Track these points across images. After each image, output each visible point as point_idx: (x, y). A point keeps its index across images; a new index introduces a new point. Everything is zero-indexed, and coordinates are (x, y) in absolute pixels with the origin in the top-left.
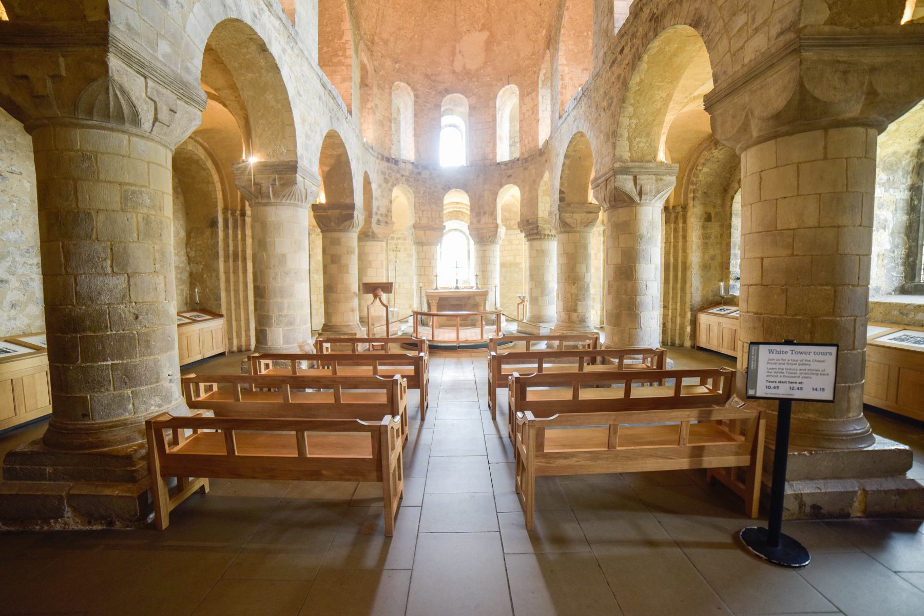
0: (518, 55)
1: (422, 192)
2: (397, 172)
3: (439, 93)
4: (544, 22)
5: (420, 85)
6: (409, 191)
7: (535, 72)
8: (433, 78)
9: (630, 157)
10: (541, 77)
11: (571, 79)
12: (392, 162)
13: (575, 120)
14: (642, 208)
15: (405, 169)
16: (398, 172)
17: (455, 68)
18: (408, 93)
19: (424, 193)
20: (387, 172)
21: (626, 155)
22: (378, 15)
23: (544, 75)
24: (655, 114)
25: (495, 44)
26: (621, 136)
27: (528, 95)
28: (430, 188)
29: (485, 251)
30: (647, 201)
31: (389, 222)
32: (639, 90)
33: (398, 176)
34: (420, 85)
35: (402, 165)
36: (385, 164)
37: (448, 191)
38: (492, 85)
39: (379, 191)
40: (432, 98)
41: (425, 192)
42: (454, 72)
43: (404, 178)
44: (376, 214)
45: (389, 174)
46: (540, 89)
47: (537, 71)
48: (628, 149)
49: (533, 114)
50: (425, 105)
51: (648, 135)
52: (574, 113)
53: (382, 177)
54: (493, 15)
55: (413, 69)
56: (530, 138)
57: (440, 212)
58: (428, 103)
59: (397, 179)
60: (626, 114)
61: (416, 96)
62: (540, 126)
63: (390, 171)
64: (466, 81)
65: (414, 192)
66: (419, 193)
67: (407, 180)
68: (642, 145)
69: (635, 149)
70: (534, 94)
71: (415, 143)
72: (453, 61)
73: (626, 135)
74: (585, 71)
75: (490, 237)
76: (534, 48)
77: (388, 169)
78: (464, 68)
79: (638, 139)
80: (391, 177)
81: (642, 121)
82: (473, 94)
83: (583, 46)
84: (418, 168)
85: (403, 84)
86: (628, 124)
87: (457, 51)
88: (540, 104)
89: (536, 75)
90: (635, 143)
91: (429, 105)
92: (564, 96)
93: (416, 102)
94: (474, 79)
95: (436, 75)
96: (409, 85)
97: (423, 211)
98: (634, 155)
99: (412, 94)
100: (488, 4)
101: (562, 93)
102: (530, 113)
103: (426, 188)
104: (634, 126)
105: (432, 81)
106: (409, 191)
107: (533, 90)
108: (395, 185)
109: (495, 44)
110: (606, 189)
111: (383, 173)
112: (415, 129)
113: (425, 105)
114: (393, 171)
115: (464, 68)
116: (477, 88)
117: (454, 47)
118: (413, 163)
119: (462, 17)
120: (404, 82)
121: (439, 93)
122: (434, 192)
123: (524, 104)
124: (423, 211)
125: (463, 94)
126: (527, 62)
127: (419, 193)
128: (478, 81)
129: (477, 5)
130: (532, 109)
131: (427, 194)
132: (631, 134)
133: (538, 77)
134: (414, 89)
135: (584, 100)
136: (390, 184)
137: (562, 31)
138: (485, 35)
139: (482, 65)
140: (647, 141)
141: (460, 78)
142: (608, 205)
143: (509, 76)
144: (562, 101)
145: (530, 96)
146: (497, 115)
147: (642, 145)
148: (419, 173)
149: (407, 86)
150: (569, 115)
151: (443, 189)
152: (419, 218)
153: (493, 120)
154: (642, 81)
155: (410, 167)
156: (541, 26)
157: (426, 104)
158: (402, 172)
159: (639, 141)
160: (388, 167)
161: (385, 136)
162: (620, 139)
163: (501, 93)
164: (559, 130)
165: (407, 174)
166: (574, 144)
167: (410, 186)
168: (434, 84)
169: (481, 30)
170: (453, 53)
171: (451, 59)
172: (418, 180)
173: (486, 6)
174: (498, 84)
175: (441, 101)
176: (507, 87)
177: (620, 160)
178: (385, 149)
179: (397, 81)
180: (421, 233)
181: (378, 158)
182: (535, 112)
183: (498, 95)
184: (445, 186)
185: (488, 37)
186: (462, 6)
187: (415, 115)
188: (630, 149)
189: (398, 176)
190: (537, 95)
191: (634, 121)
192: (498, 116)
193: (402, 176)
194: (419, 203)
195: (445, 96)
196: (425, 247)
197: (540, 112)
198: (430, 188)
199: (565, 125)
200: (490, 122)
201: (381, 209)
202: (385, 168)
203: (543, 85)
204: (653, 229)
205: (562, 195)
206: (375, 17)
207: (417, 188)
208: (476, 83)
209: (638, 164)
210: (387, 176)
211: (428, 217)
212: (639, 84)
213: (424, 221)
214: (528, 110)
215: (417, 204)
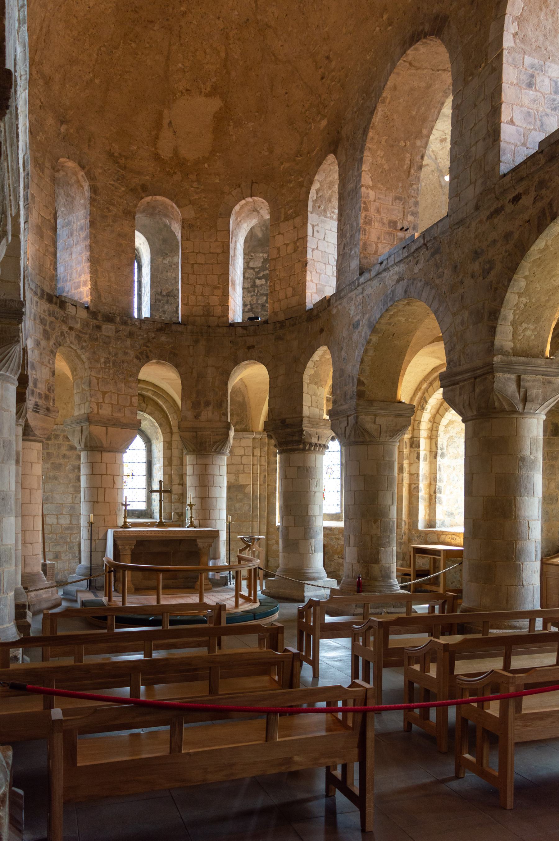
0: (271, 151)
1: (102, 360)
2: (63, 321)
3: (131, 190)
4: (325, 107)
5: (100, 171)
6: (79, 357)
7: (301, 185)
8: (122, 161)
9: (512, 349)
10: (313, 195)
11: (378, 211)
12: (56, 304)
13: (398, 281)
14: (526, 420)
15: (74, 318)
16: (64, 321)
17: (160, 152)
18: (78, 181)
19: (105, 362)
20: (49, 319)
21: (509, 345)
22: (41, 29)
23: (317, 193)
24: (550, 293)
25: (231, 124)
26: (505, 319)
27: (287, 219)
28: (116, 354)
29: (206, 465)
30: (532, 411)
31: (52, 409)
32: (539, 259)
33: (65, 328)
34: (100, 171)
35: (71, 310)
36: (45, 305)
37: (147, 362)
38: (222, 193)
39: (36, 352)
40: (121, 197)
41: (107, 361)
42: (157, 157)
43: (73, 333)
44: (33, 393)
45: (50, 325)
46: (309, 214)
47: (305, 184)
48: (511, 337)
49: (295, 250)
50: (107, 208)
51: (537, 321)
52: (396, 269)
53: (40, 328)
54: (233, 74)
55: (90, 140)
56: (290, 289)
57: (131, 396)
58: (113, 205)
59: (62, 334)
60: (516, 290)
61: (94, 190)
62: (308, 272)
63: (53, 319)
64: (177, 177)
65: (89, 359)
66: (98, 361)
67: (78, 337)
68: (528, 333)
69: (520, 338)
70: (298, 220)
71: (91, 272)
72: (157, 137)
73: (511, 317)
74: (397, 201)
75: (215, 443)
76: (301, 143)
77: (49, 315)
78: (176, 151)
79: (524, 325)
80: (54, 329)
81: (533, 301)
82: (190, 201)
83: (397, 162)
84: (96, 319)
85: (70, 164)
86: (515, 303)
87: (166, 122)
88: (309, 238)
89: (304, 189)
90: (521, 329)
91: (114, 210)
92: (367, 236)
93: (93, 201)
94: (193, 177)
95: (126, 158)
96: (83, 167)
97: (104, 393)
98: (518, 345)
99: (86, 186)
100: (227, 54)
101: (365, 230)
102: (290, 249)
103: (110, 354)
104: (522, 306)
105: (120, 167)
106: (79, 357)
107: (298, 215)
108: (60, 345)
109: (231, 124)
110: (474, 390)
111: (43, 321)
112: (91, 249)
113: (107, 208)
114: (57, 319)
115: (176, 151)
116: (197, 193)
117: (160, 114)
118: (87, 308)
119: (180, 65)
120: (74, 160)
121: (131, 190)
122: (123, 362)
123: (279, 234)
124: (104, 393)
125: (172, 199)
126: (287, 165)
127: (98, 361)
128: (198, 181)
129: (208, 51)
130: (295, 243)
131: (111, 364)
132: (517, 317)
133: (308, 193)
134: (90, 177)
135: (424, 254)
136: (52, 342)
137: (371, 134)
138: (216, 104)
139: (207, 155)
140: (536, 328)
141: (167, 170)
142: (475, 413)
143: (253, 183)
144: (365, 244)
145: (291, 222)
146: (231, 244)
147: (528, 333)
148: (99, 327)
149: (78, 168)
150: (386, 269)
151: (137, 357)
152: (98, 404)
153: (223, 252)
154: (546, 248)
155: (83, 314)
156: (319, 113)
157: (111, 208)
158: (71, 323)
159: (526, 328)
160: (49, 311)
161: (44, 255)
162: (503, 323)
163: (237, 208)
164: (359, 288)
165: (78, 326)
166: (391, 313)
167: (82, 348)
168: (124, 173)
169: (209, 95)
170: (158, 125)
171: (153, 133)
172: (97, 339)
173: (223, 55)
174: (234, 193)
175: (136, 206)
176: (249, 199)
177: (502, 352)
178: (44, 278)
179: (63, 157)
180: (98, 430)
181: (36, 293)
182: (300, 249)
183: (233, 212)
184: (141, 353)
185: (221, 109)
186: (181, 44)
187: (92, 224)
188: (514, 338)
189: (65, 328)
190: (305, 224)
191: (524, 300)
192: (232, 246)
193: (71, 329)
194: (98, 379)
195: (142, 198)
196: (105, 455)
197: (309, 251)
198: (116, 354)
199: (375, 283)
200: (218, 254)
201: (39, 385)
202: (44, 311)
203: (314, 207)
204: (537, 449)
205: (361, 388)
206: (38, 31)
207: (94, 353)
208: (195, 185)
209: (522, 359)
210: (47, 328)
211: (112, 404)
212: (541, 251)
213: (106, 411)
214: (287, 245)
215: (94, 381)
